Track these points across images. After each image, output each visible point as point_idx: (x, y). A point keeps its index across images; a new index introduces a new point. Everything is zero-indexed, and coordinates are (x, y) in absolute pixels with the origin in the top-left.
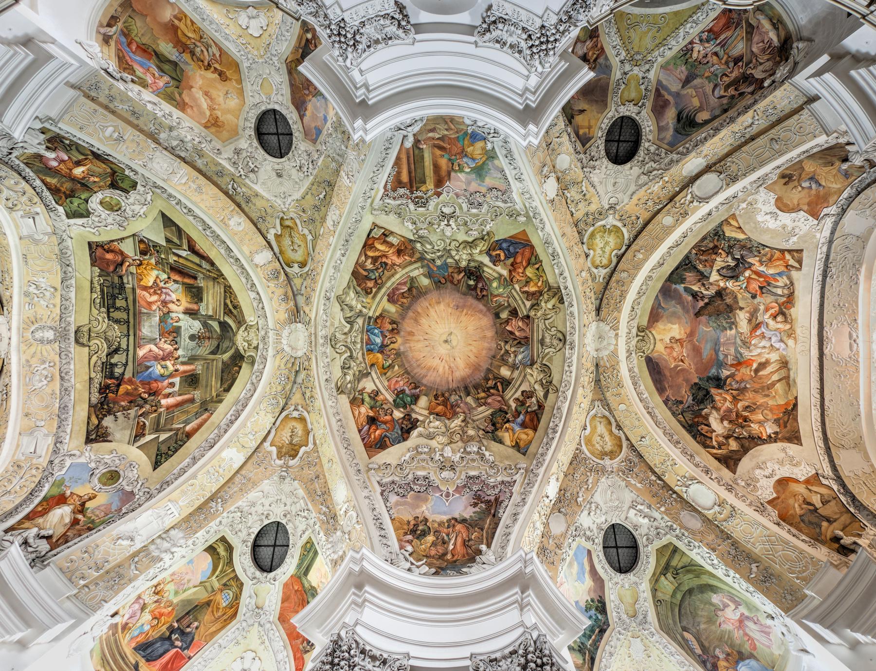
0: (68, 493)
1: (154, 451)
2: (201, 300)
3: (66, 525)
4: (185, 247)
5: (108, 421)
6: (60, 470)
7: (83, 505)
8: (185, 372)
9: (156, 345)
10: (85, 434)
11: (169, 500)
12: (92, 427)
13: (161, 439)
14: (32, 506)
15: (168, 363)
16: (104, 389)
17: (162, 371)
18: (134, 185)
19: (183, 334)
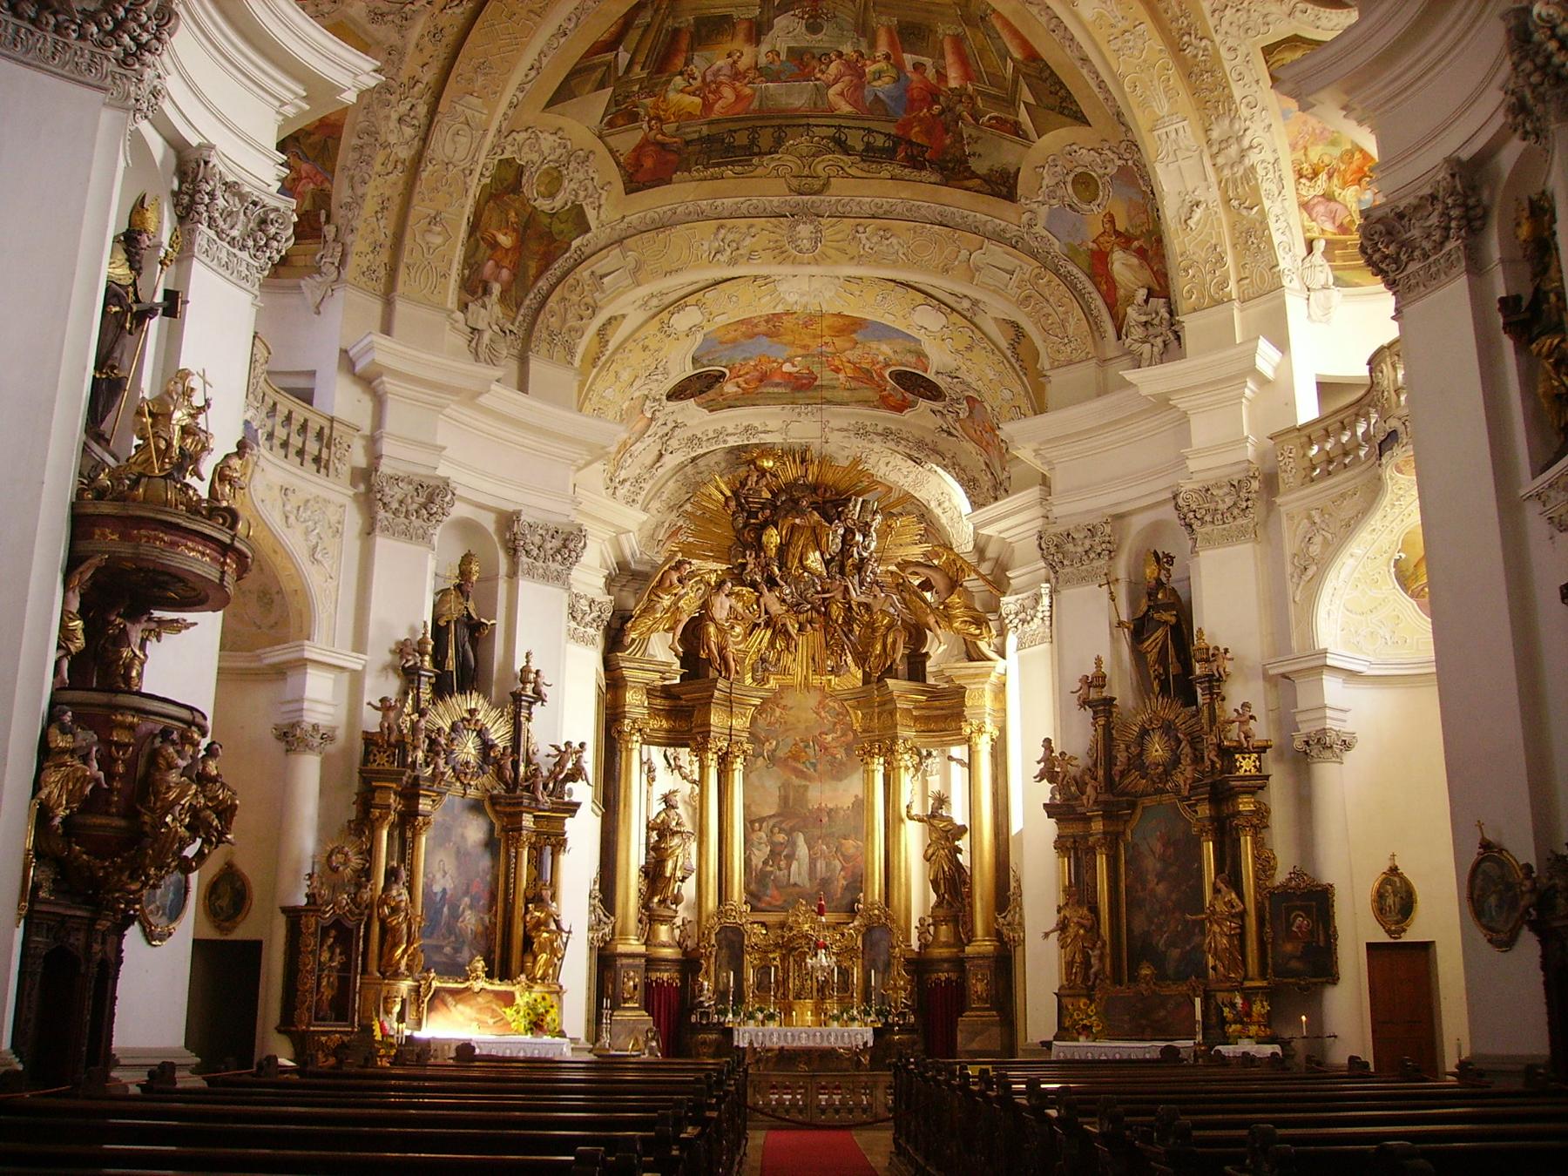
0: (1091, 245)
1: (1053, 116)
2: (727, 18)
4: (610, 56)
5: (979, 166)
7: (1118, 234)
8: (892, 44)
9: (829, 87)
11: (1152, 130)
13: (1031, 100)
14: (1096, 295)
15: (870, 68)
16: (915, 163)
17: (886, 79)
18: (509, 162)
19: (805, 44)
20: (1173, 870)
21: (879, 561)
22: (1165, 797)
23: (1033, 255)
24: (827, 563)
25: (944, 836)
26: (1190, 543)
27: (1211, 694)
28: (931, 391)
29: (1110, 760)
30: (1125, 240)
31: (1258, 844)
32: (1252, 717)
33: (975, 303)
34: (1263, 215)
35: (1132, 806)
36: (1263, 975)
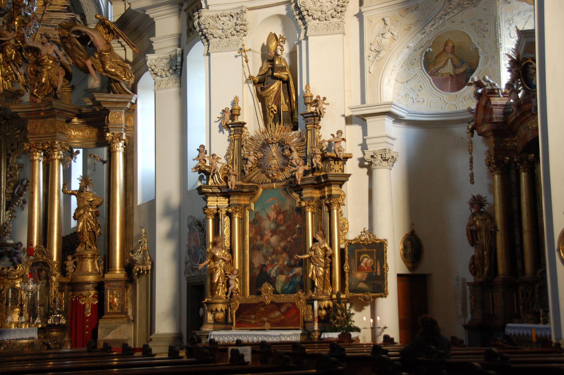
20: (283, 228)
32: (344, 139)
35: (257, 188)
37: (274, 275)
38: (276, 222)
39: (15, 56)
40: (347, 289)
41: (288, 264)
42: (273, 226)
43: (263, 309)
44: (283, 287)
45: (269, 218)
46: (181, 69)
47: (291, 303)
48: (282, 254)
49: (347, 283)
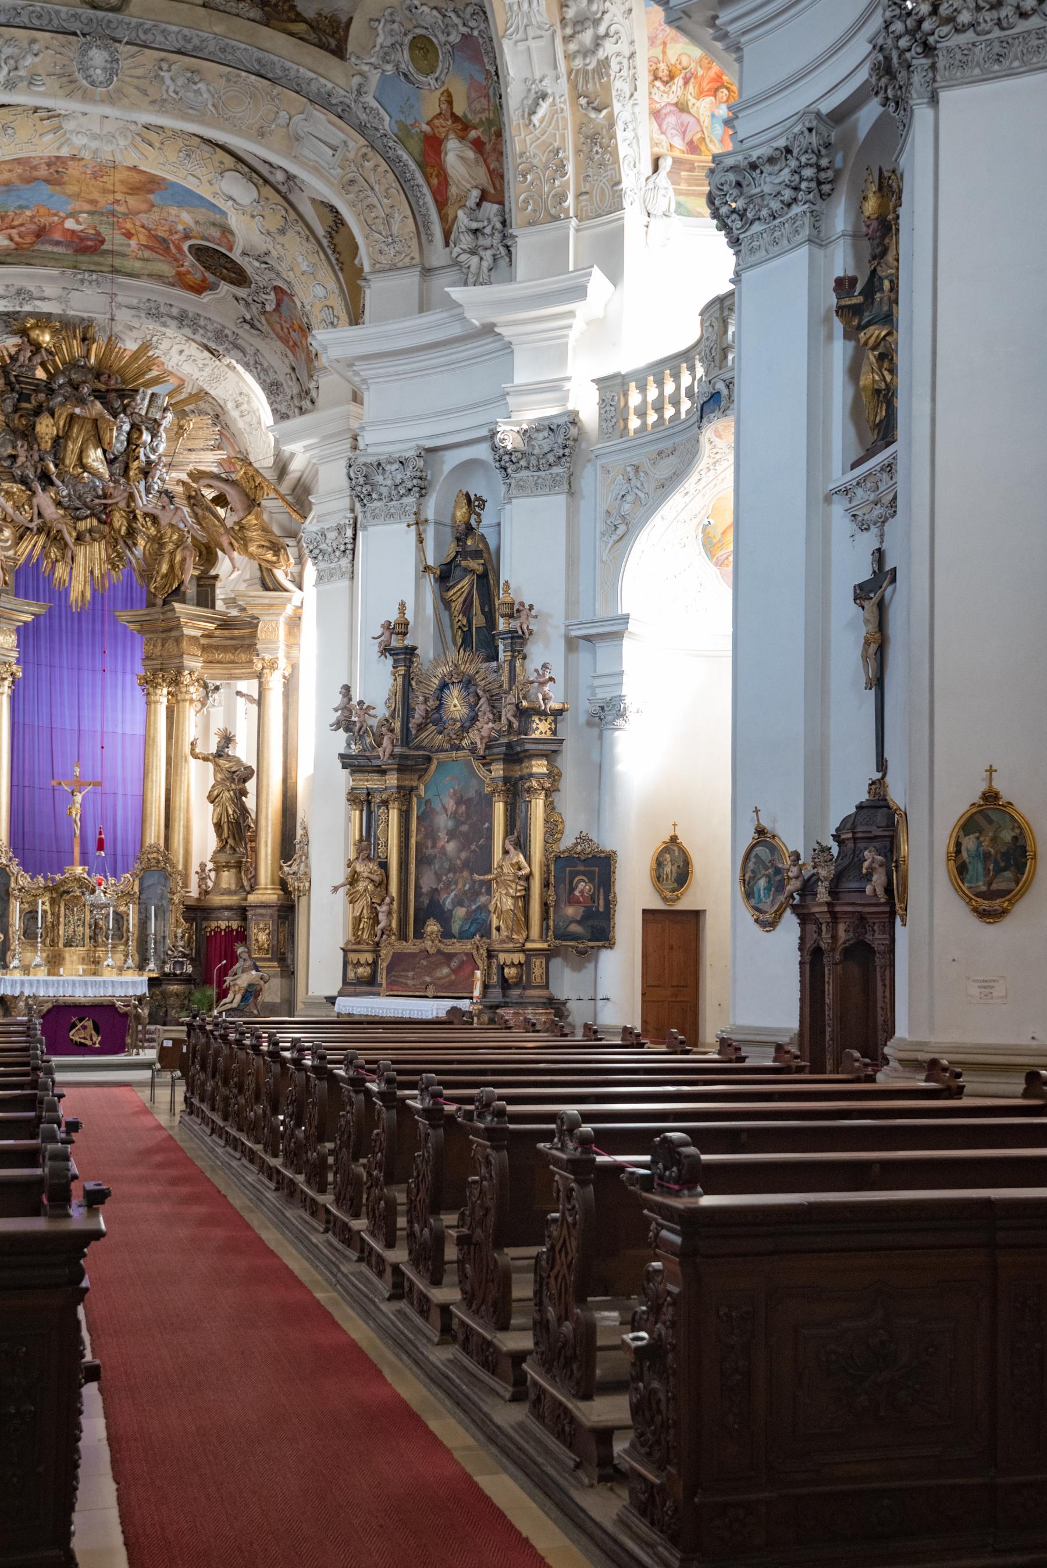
0: (426, 128)
3: (477, 161)
6: (381, 120)
10: (323, 52)
12: (312, 36)
14: (426, 190)
20: (464, 828)
21: (169, 466)
22: (461, 753)
23: (361, 129)
24: (110, 462)
25: (234, 779)
26: (503, 488)
27: (513, 651)
28: (239, 277)
29: (407, 710)
30: (462, 126)
31: (550, 807)
33: (290, 177)
34: (611, 124)
35: (429, 759)
36: (543, 937)
37: (450, 908)
38: (455, 817)
39: (127, 529)
40: (550, 933)
41: (470, 889)
42: (450, 824)
43: (425, 963)
44: (462, 926)
45: (445, 809)
46: (353, 550)
47: (467, 954)
48: (462, 872)
49: (551, 923)
